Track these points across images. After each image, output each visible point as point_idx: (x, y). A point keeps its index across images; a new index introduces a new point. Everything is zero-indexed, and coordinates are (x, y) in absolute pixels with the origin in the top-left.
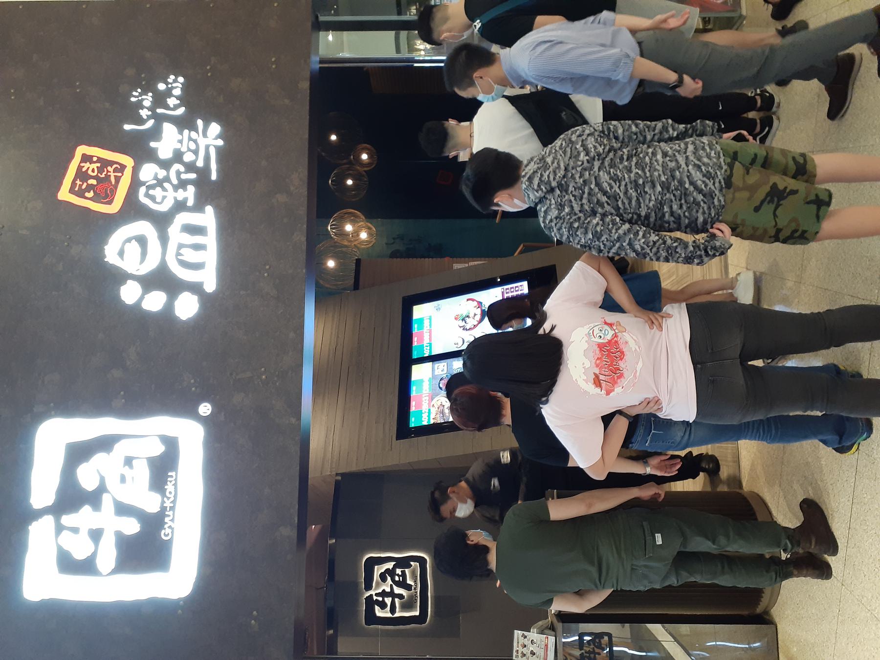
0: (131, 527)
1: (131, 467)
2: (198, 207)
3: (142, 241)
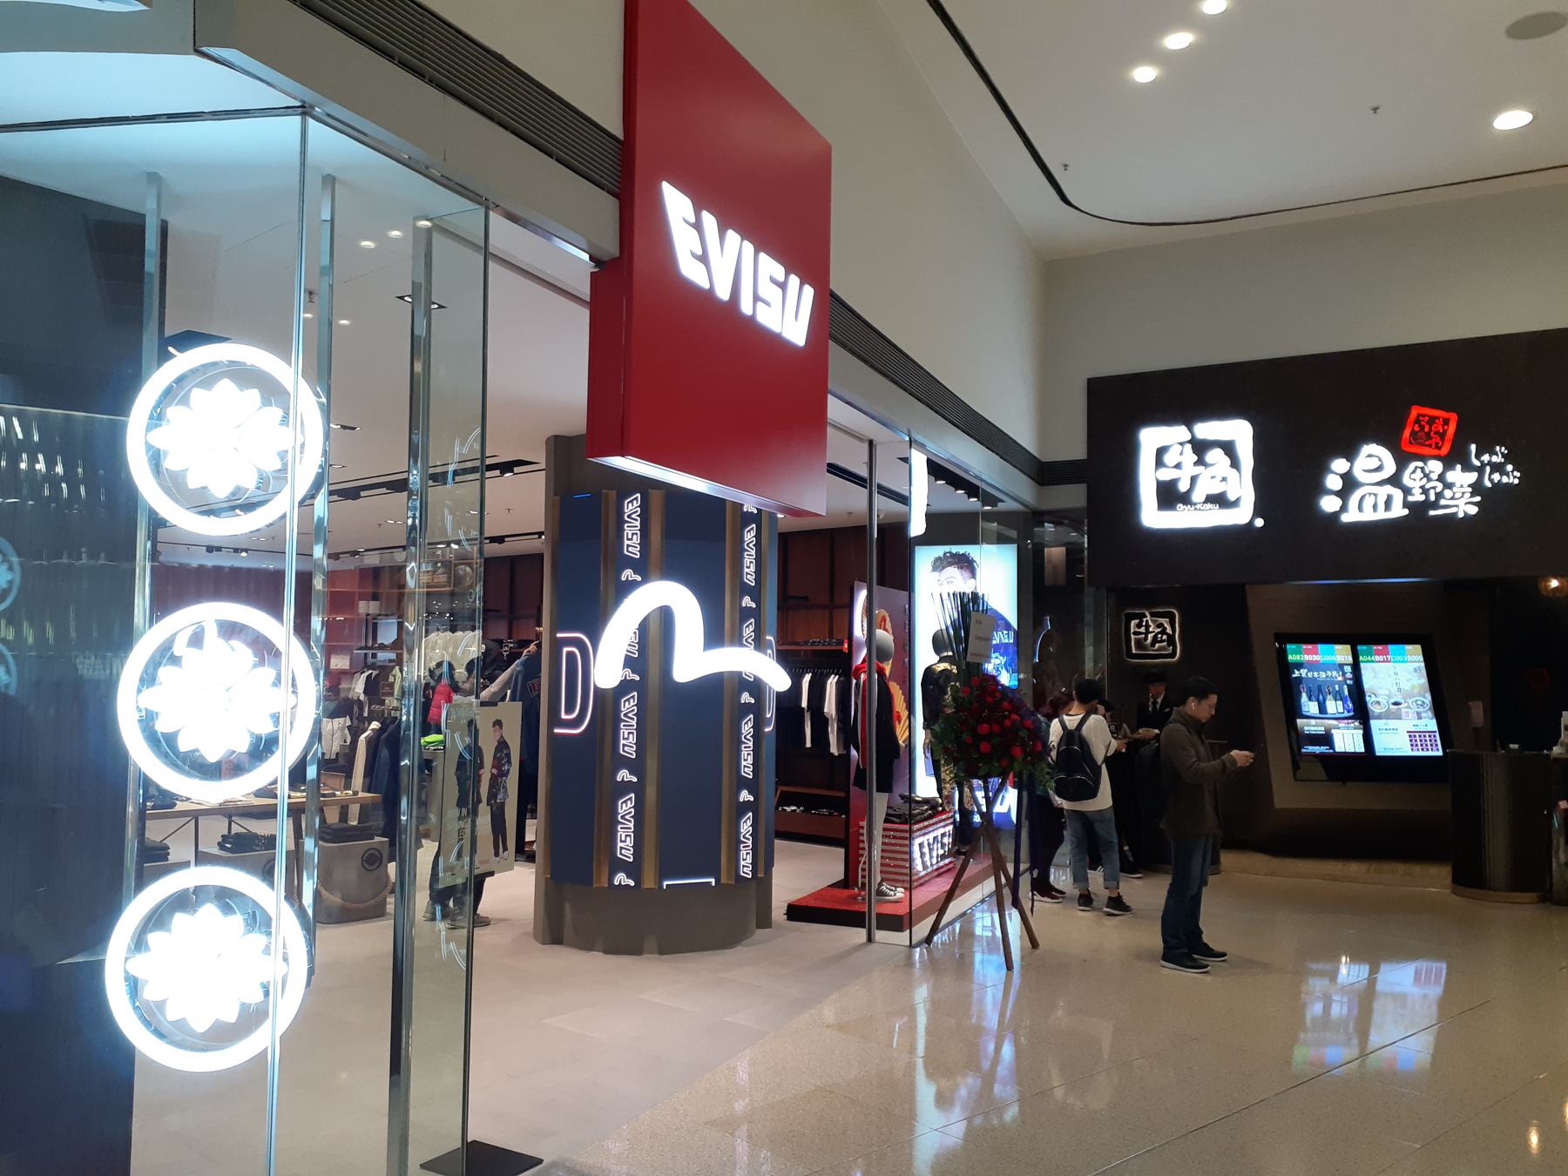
0: (1183, 487)
1: (1221, 481)
2: (1406, 504)
3: (1379, 469)
